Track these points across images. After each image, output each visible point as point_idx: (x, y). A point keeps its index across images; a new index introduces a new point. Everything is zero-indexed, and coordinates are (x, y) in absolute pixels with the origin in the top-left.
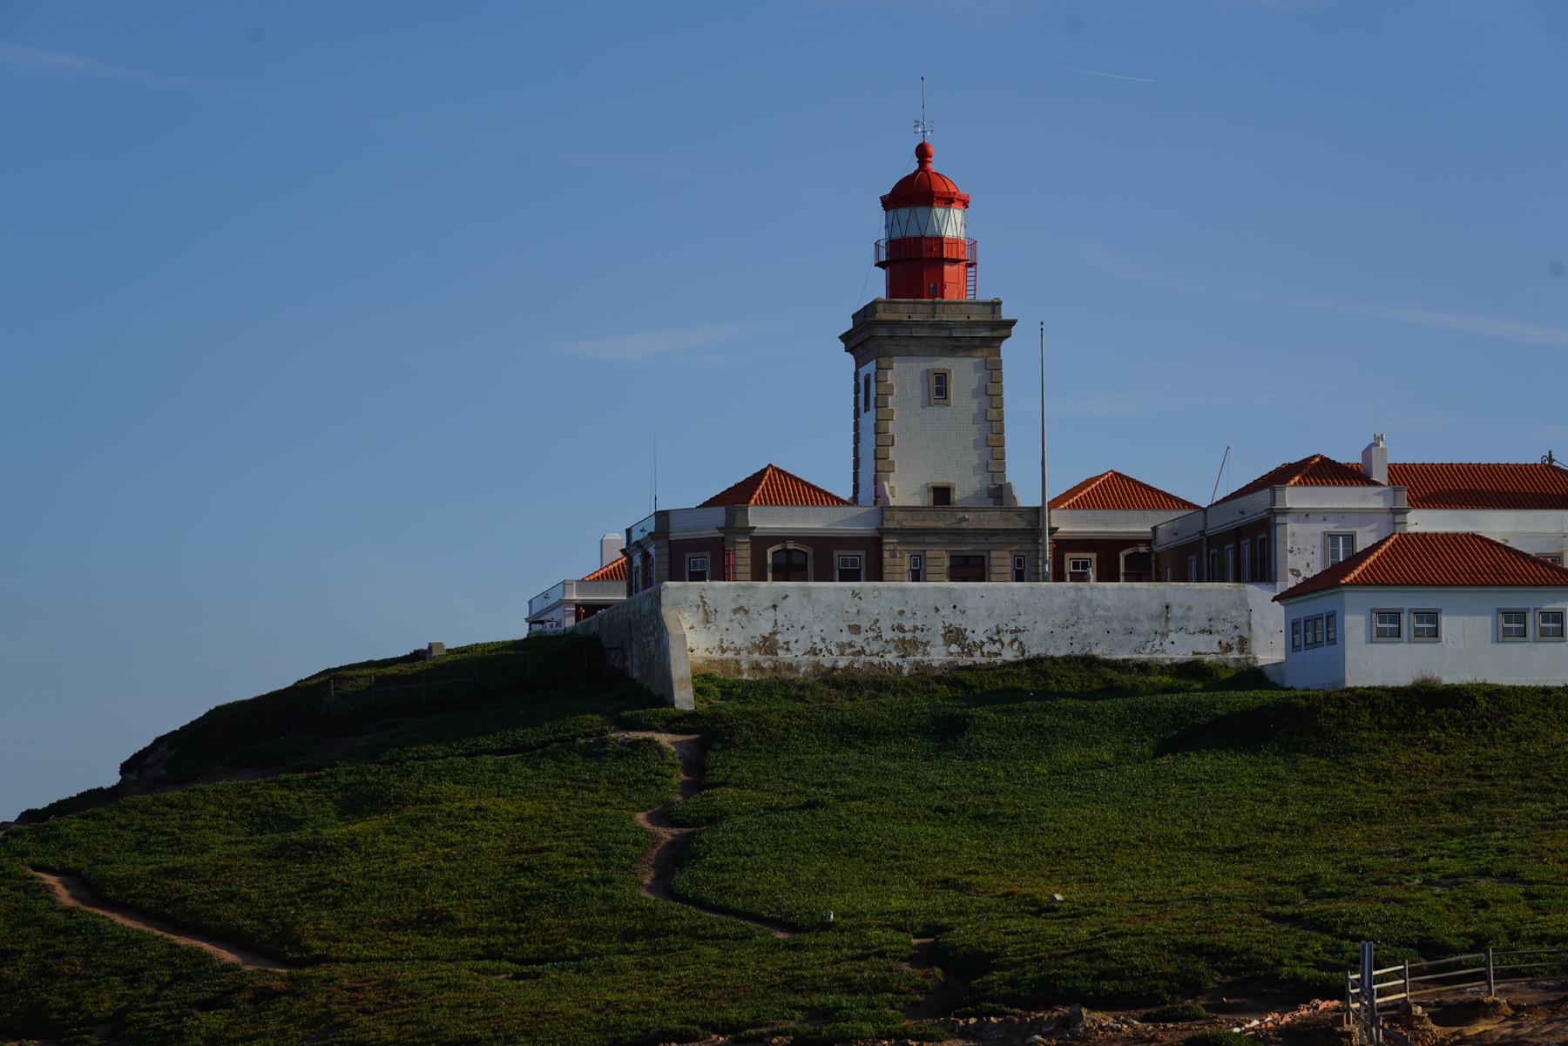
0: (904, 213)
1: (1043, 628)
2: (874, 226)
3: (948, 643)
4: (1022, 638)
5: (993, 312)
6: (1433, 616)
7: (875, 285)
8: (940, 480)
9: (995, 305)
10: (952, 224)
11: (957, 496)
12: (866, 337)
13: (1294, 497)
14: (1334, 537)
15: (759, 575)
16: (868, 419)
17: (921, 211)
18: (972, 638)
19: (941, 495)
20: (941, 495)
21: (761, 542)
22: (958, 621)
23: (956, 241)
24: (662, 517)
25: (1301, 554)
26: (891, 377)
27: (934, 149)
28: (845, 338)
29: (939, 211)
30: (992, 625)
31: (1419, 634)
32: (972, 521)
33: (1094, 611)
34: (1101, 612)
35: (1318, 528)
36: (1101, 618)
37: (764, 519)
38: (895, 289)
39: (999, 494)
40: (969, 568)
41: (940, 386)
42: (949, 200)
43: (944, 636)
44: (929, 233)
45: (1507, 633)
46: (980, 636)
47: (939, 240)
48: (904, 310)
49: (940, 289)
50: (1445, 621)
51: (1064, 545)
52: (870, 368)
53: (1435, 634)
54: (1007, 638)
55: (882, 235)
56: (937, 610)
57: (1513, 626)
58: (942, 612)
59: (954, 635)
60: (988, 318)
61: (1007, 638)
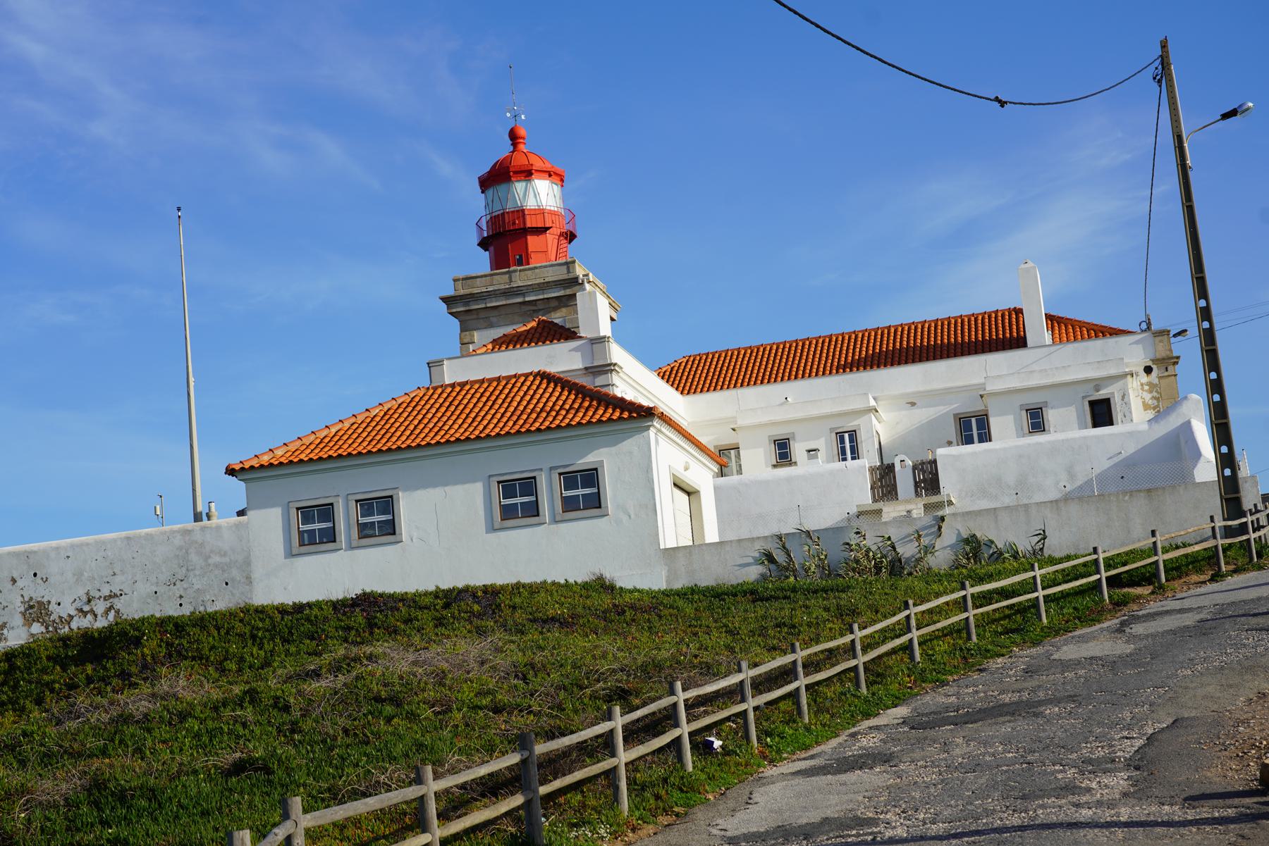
0: (490, 192)
1: (144, 589)
3: (28, 622)
4: (118, 604)
5: (569, 272)
6: (387, 504)
9: (569, 265)
10: (541, 195)
17: (502, 188)
18: (57, 612)
22: (38, 592)
23: (541, 212)
27: (522, 132)
29: (519, 186)
30: (81, 592)
31: (365, 531)
33: (207, 558)
34: (216, 559)
36: (216, 566)
42: (527, 174)
43: (23, 614)
44: (510, 207)
45: (508, 513)
46: (68, 609)
47: (521, 213)
49: (523, 259)
50: (408, 508)
53: (390, 528)
54: (100, 607)
56: (14, 581)
57: (516, 502)
58: (20, 583)
59: (36, 610)
60: (566, 277)
61: (100, 607)
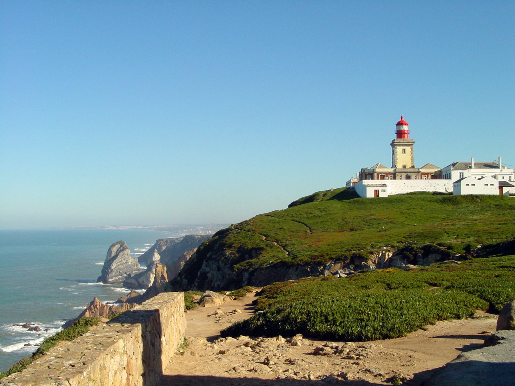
2: (395, 128)
8: (404, 164)
11: (407, 167)
15: (378, 179)
19: (404, 167)
21: (378, 174)
26: (397, 150)
28: (391, 144)
32: (409, 170)
37: (378, 170)
38: (398, 138)
40: (408, 177)
41: (404, 151)
51: (423, 173)
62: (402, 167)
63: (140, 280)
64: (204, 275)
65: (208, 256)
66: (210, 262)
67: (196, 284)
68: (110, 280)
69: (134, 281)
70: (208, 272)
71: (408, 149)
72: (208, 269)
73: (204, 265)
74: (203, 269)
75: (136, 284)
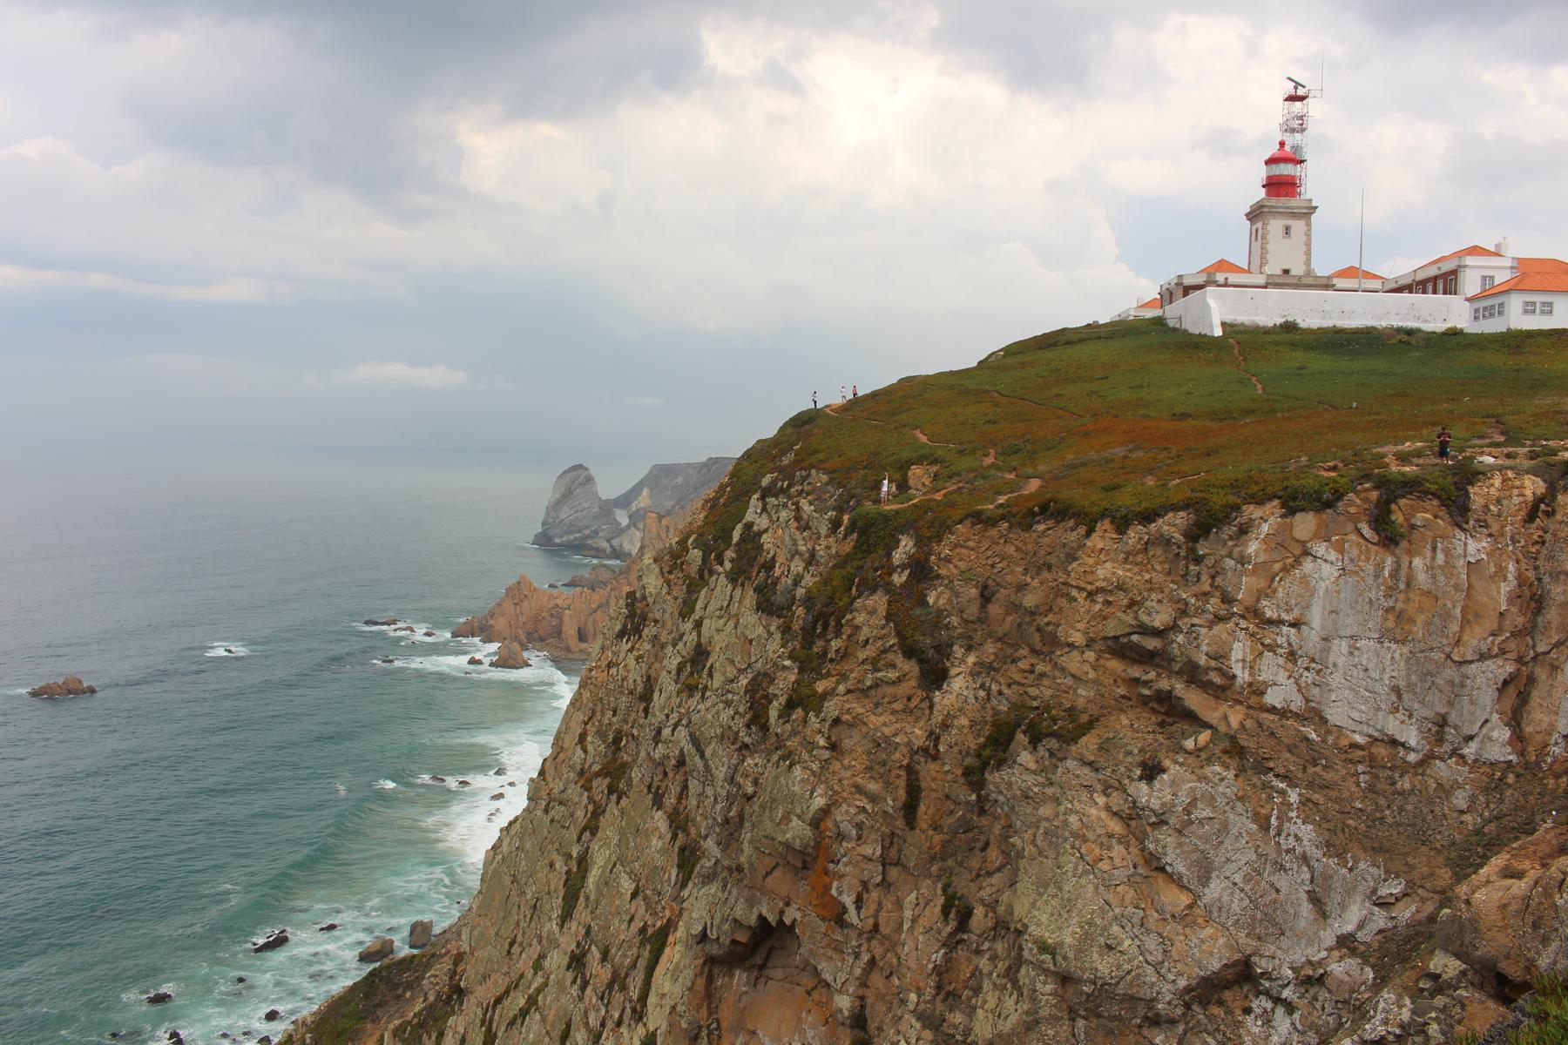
0: (1274, 166)
2: (1261, 173)
7: (1262, 193)
12: (1255, 214)
13: (1470, 260)
14: (1484, 278)
16: (1257, 246)
20: (1286, 272)
24: (1180, 277)
25: (1471, 283)
35: (1479, 274)
38: (1269, 194)
39: (1309, 273)
48: (1274, 201)
52: (1259, 225)
55: (1264, 175)
62: (1279, 272)
63: (615, 542)
64: (752, 538)
65: (765, 481)
66: (772, 500)
67: (728, 565)
68: (557, 541)
69: (605, 545)
70: (766, 531)
71: (1298, 226)
72: (762, 522)
73: (751, 510)
74: (749, 526)
75: (609, 550)
